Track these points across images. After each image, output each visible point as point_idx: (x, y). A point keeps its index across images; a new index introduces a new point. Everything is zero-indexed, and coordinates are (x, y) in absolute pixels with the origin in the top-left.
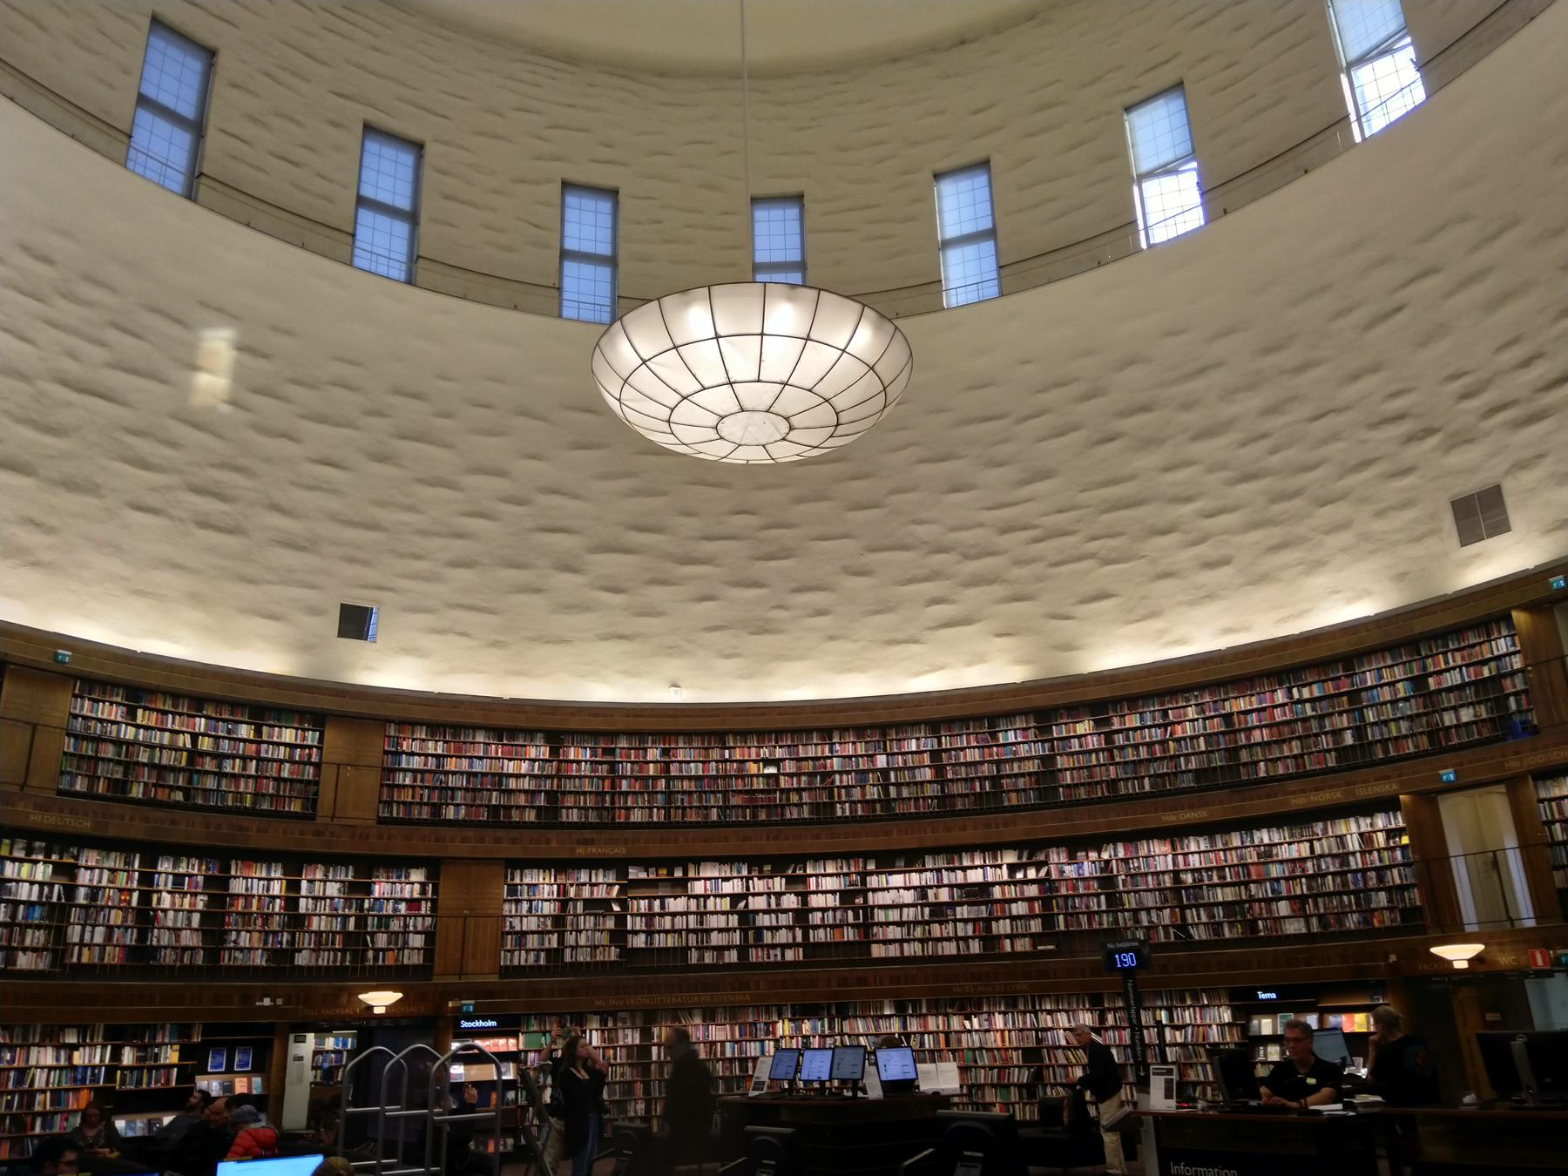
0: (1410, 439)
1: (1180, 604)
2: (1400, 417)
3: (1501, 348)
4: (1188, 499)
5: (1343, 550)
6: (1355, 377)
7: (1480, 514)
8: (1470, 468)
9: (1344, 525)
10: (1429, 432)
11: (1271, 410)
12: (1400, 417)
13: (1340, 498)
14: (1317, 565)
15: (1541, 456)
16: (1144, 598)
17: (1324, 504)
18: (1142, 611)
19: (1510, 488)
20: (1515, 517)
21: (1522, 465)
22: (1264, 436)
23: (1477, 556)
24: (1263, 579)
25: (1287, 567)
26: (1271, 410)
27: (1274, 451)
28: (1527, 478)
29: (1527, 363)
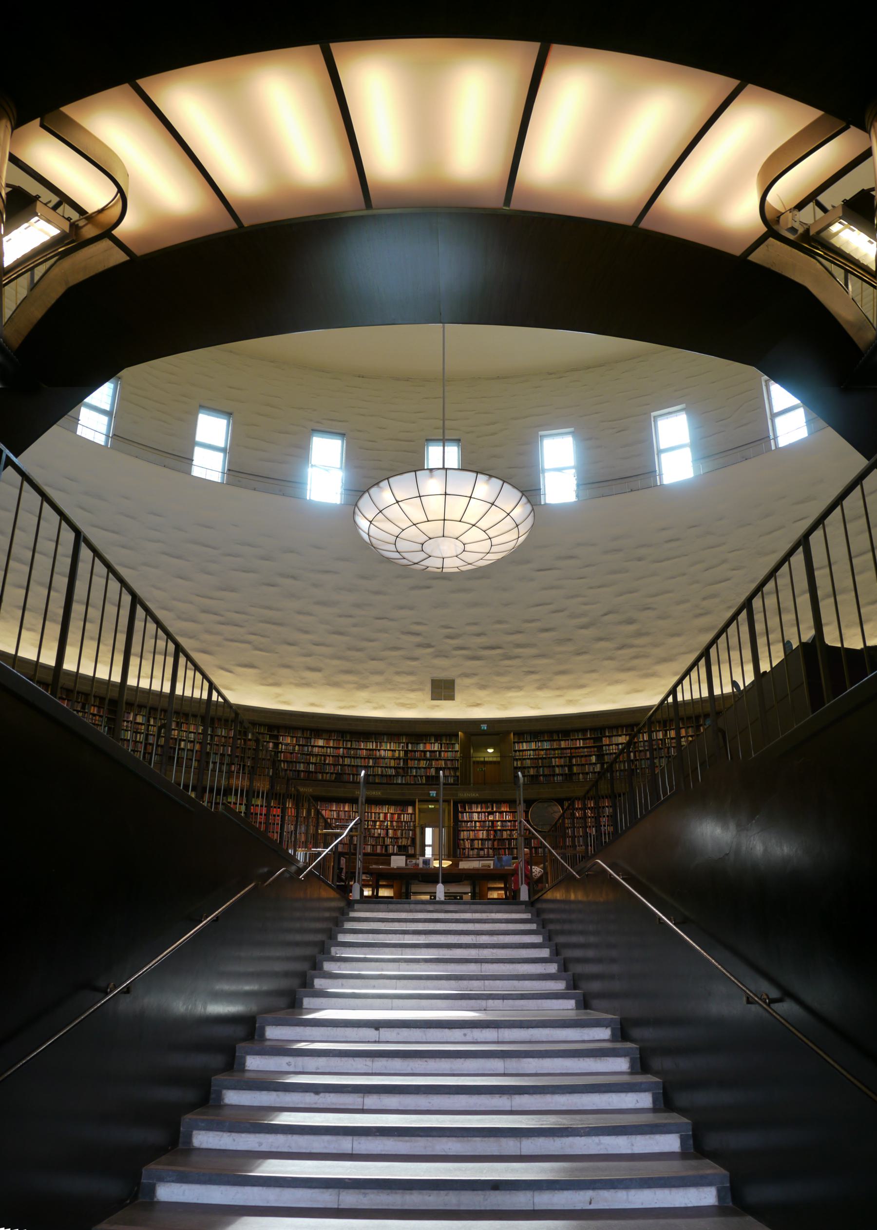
0: (419, 645)
1: (291, 683)
2: (417, 634)
3: (468, 624)
4: (306, 632)
5: (377, 684)
6: (401, 608)
7: (443, 689)
8: (444, 669)
9: (381, 673)
10: (429, 646)
11: (358, 606)
12: (417, 634)
13: (381, 660)
14: (362, 687)
15: (475, 675)
16: (273, 674)
17: (373, 659)
18: (270, 681)
19: (458, 682)
20: (458, 696)
21: (466, 675)
22: (350, 616)
23: (438, 706)
24: (336, 685)
25: (349, 682)
26: (358, 606)
27: (355, 625)
28: (468, 681)
29: (479, 635)
